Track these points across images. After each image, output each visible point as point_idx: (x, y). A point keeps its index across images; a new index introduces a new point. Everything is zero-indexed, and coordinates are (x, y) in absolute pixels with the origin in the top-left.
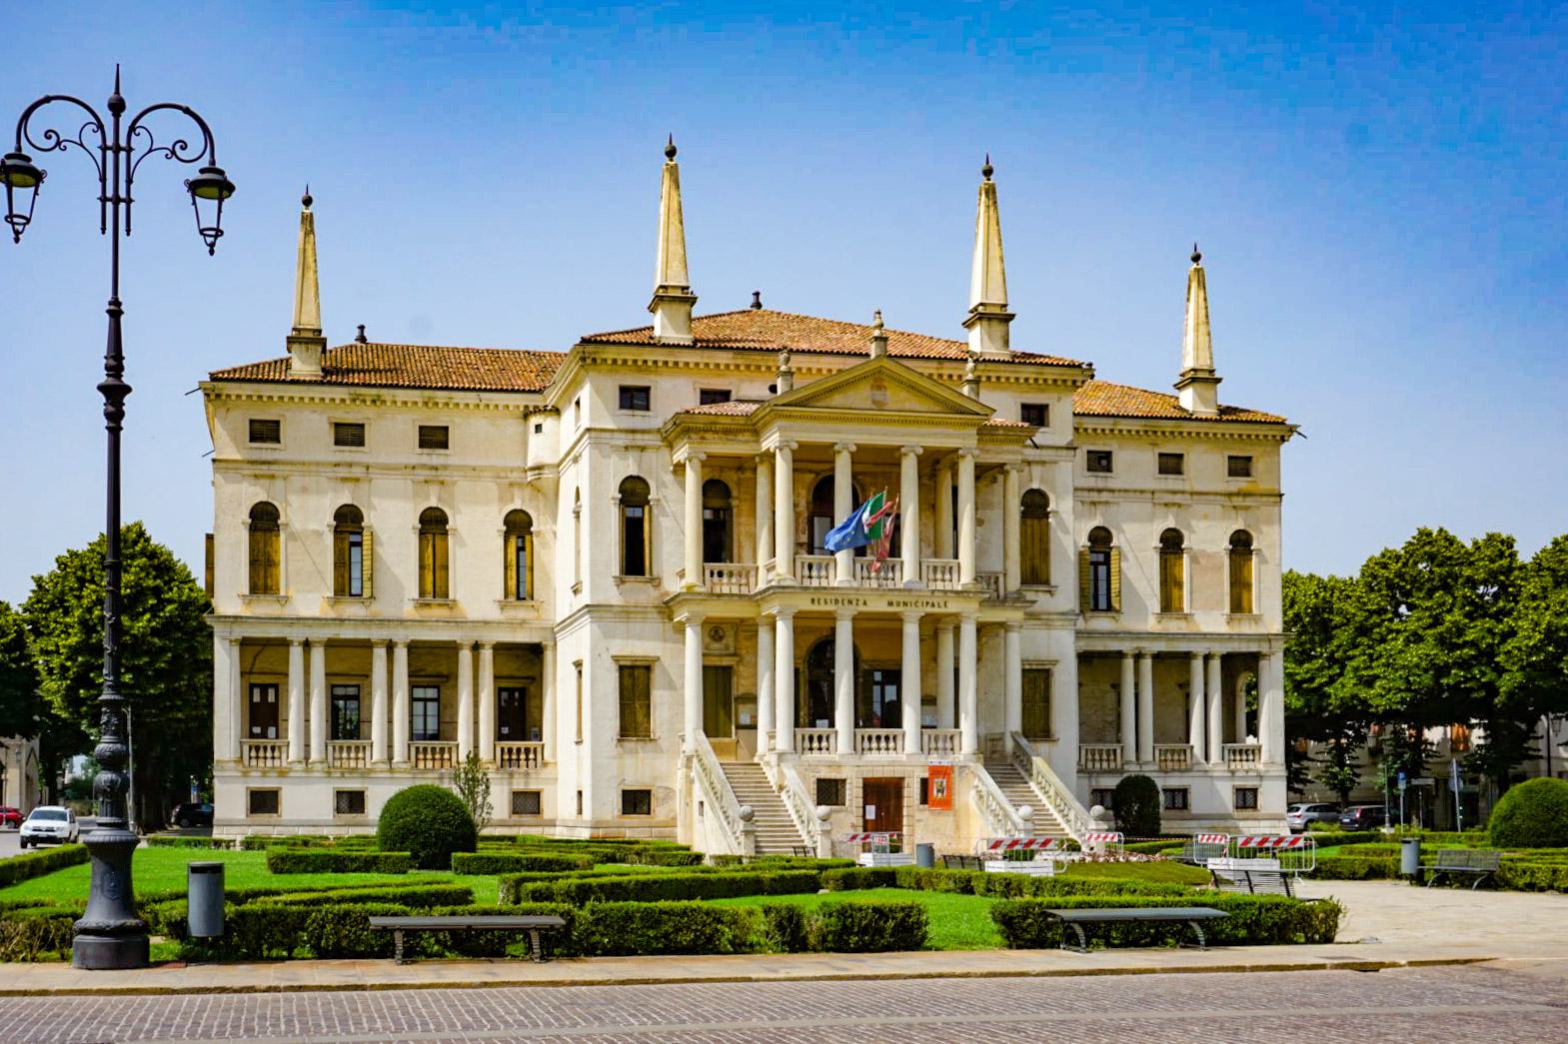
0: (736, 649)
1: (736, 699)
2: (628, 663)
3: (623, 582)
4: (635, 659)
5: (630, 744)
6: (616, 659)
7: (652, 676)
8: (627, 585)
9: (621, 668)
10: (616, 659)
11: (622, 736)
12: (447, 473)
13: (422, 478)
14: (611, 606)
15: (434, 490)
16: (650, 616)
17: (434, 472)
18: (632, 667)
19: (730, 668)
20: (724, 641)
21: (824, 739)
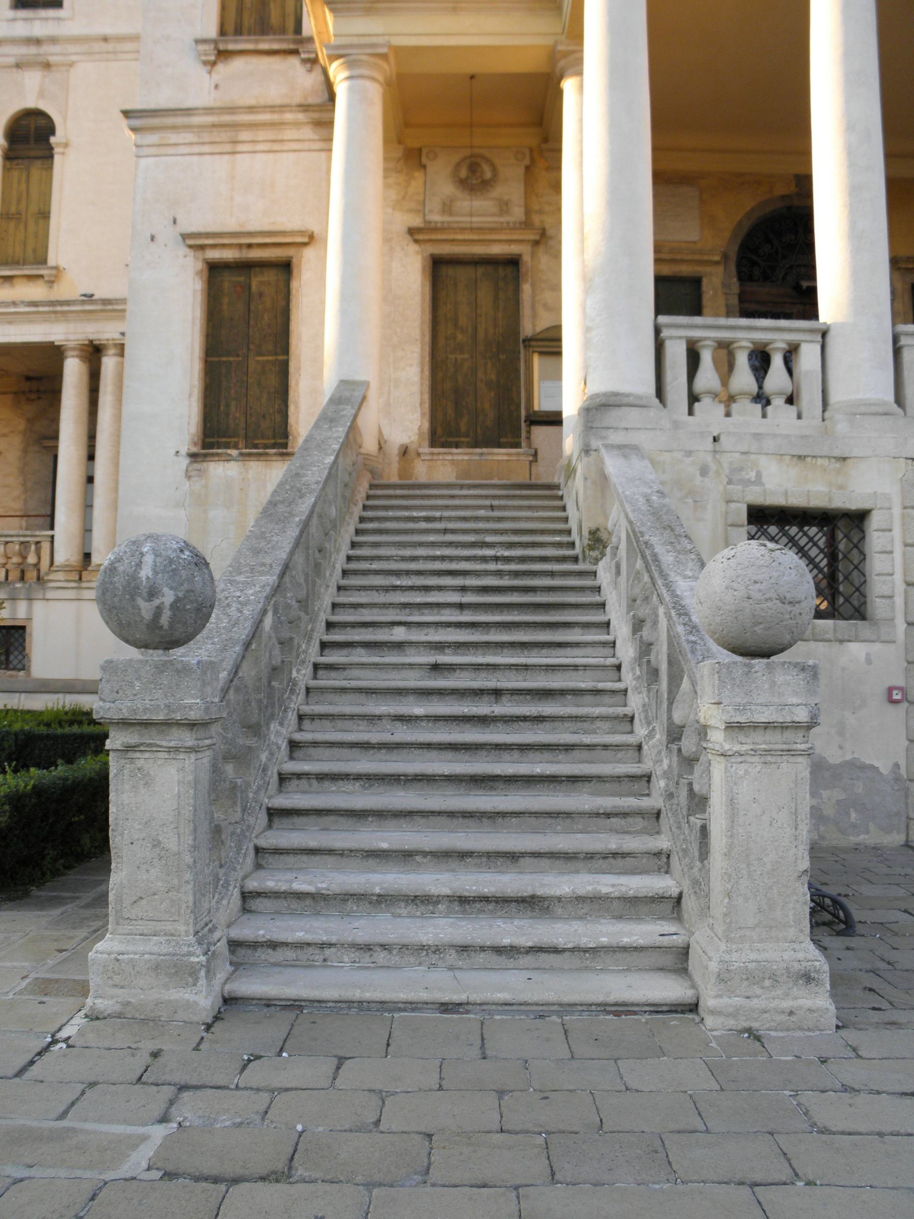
0: (528, 212)
1: (524, 341)
2: (228, 255)
3: (223, 55)
4: (243, 239)
5: (225, 471)
6: (195, 242)
7: (294, 284)
8: (238, 64)
9: (214, 269)
10: (195, 242)
11: (205, 445)
12: (57, 49)
13: (12, 60)
14: (188, 111)
15: (32, 80)
16: (290, 134)
17: (33, 50)
18: (246, 267)
19: (514, 262)
20: (498, 191)
21: (777, 361)
